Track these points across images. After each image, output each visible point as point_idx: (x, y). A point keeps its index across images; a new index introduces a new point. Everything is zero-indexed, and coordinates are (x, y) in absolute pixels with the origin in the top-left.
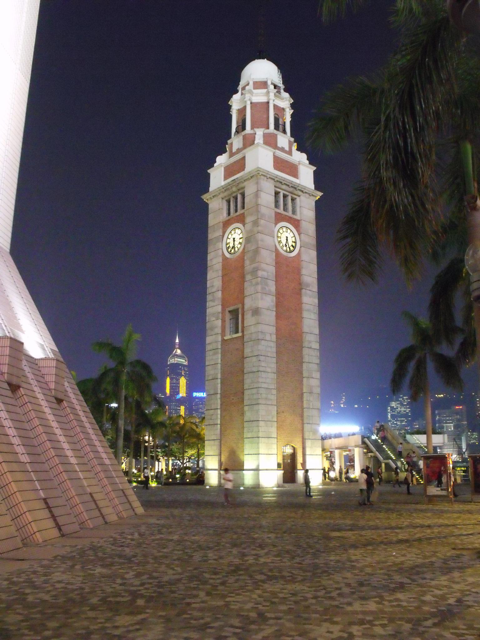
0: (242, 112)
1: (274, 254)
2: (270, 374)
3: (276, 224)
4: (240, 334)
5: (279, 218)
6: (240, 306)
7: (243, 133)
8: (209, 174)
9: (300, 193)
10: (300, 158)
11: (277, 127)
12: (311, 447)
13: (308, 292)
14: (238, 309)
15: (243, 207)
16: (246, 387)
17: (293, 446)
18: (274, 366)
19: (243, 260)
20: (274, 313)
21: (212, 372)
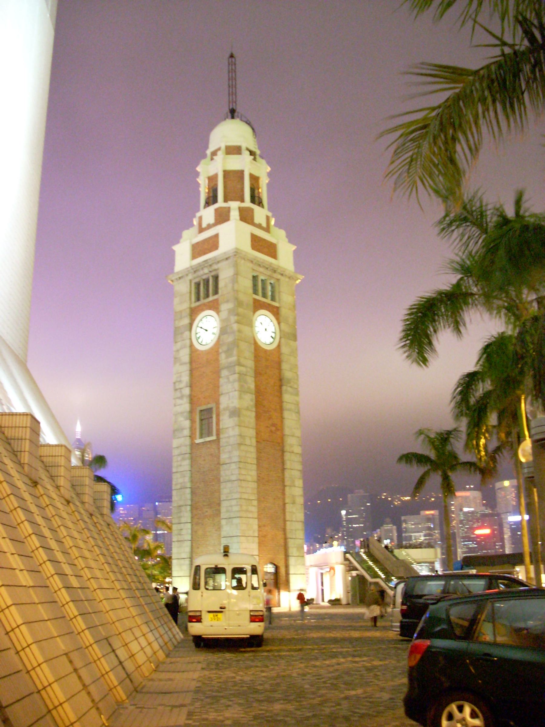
0: (212, 179)
1: (253, 347)
2: (250, 483)
3: (254, 312)
4: (214, 438)
5: (258, 306)
6: (213, 405)
7: (216, 206)
8: (174, 252)
9: (279, 277)
10: (278, 236)
11: (253, 200)
13: (289, 389)
14: (211, 409)
15: (216, 292)
16: (223, 497)
18: (254, 473)
19: (218, 353)
21: (181, 480)
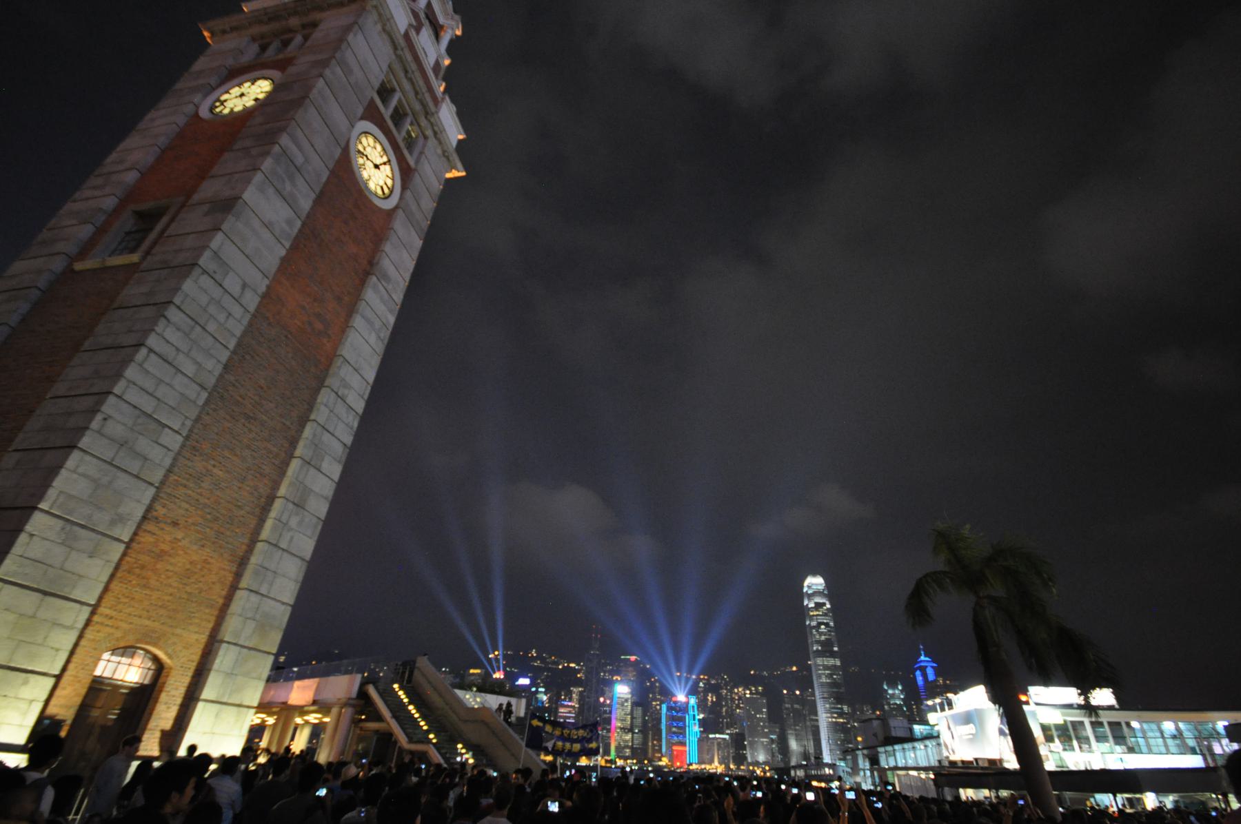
9: (429, 133)
12: (230, 675)
17: (156, 659)
20: (283, 252)
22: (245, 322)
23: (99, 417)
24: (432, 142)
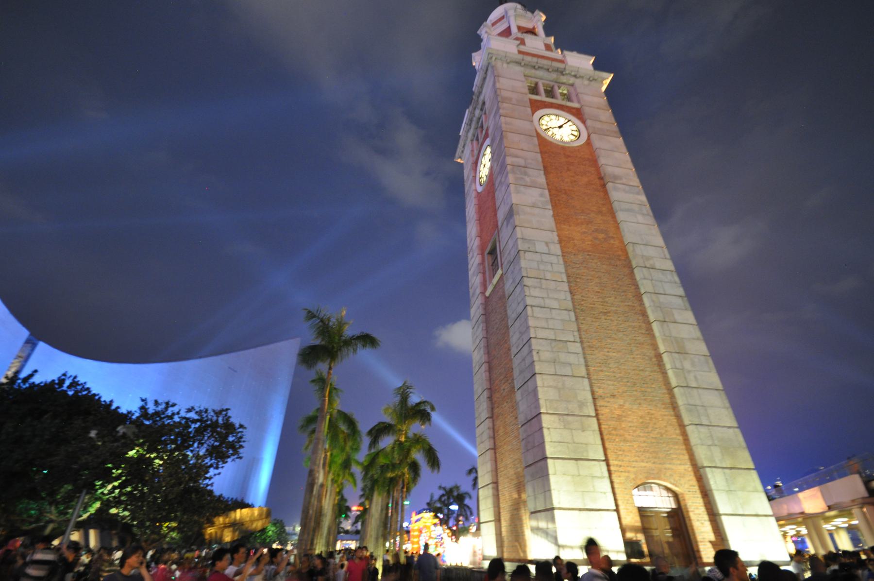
9: (572, 80)
20: (551, 212)
22: (561, 262)
23: (534, 353)
24: (578, 82)
